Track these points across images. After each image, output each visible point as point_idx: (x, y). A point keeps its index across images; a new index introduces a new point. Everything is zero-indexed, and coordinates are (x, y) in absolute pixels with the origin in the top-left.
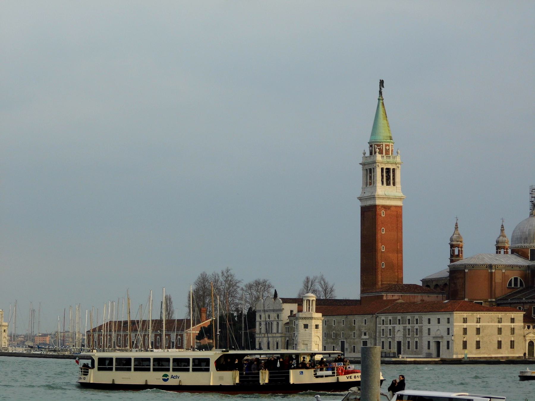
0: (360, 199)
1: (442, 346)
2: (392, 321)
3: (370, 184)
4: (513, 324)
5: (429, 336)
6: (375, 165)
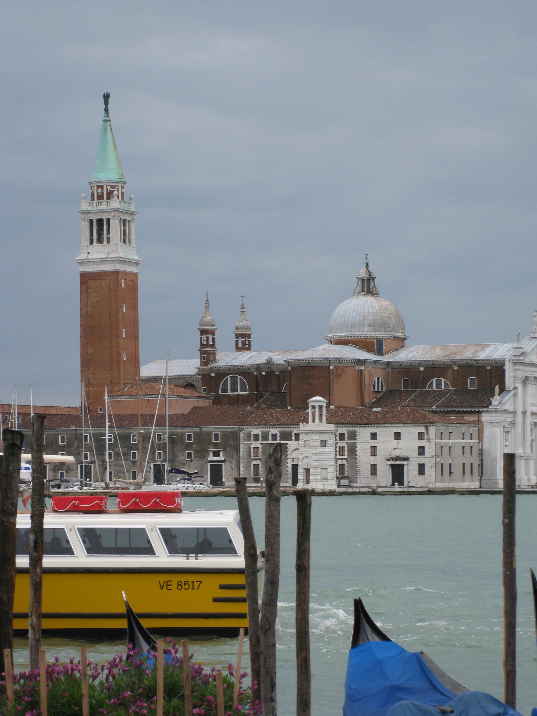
1: (408, 470)
2: (278, 436)
3: (100, 240)
4: (471, 441)
5: (374, 457)
6: (113, 213)
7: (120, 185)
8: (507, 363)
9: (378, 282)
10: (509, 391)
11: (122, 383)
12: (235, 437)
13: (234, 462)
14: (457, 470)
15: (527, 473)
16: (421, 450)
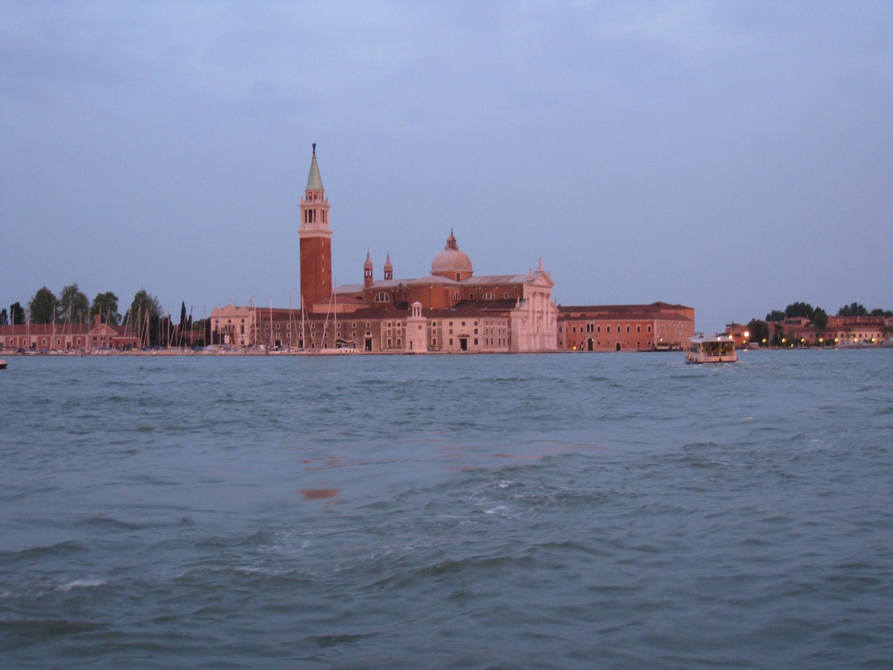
0: (300, 232)
3: (310, 221)
7: (321, 192)
8: (524, 285)
9: (458, 243)
10: (525, 300)
11: (322, 297)
12: (379, 325)
13: (378, 338)
14: (496, 342)
15: (535, 343)
16: (476, 331)
